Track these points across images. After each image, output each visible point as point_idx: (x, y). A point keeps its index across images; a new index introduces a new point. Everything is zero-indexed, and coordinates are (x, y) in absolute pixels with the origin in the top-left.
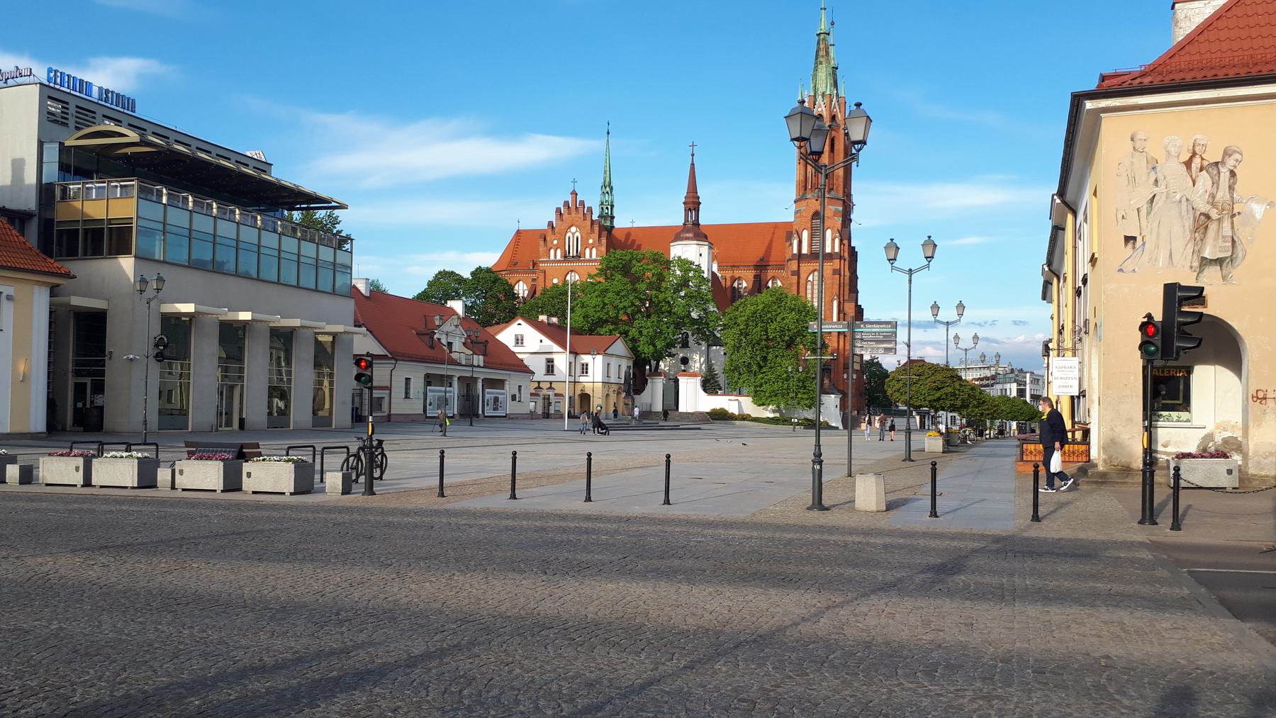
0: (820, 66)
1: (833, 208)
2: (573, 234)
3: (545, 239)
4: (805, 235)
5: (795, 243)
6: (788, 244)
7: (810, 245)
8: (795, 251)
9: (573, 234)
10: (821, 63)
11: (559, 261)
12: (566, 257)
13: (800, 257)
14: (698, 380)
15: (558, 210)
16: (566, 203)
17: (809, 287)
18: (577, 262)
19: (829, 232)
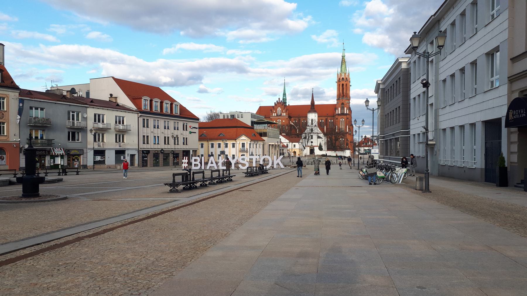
0: (343, 65)
1: (346, 102)
2: (279, 109)
3: (272, 111)
4: (339, 109)
5: (337, 111)
6: (335, 111)
7: (341, 111)
8: (337, 113)
9: (279, 109)
10: (343, 64)
11: (276, 116)
12: (277, 115)
13: (338, 114)
14: (318, 147)
15: (275, 103)
16: (277, 101)
17: (341, 122)
18: (281, 116)
19: (345, 108)
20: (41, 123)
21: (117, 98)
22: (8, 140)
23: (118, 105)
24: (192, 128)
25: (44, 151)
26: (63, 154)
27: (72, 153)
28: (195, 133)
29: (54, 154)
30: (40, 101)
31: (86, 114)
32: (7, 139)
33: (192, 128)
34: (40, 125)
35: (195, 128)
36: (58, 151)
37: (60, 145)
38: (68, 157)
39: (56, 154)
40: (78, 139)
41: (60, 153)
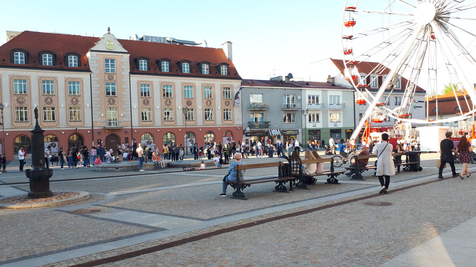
20: (259, 108)
21: (334, 78)
22: (233, 124)
23: (333, 85)
24: (416, 101)
25: (263, 132)
26: (279, 134)
27: (288, 133)
28: (422, 107)
29: (271, 135)
30: (259, 88)
31: (300, 96)
32: (215, 123)
33: (416, 101)
34: (258, 109)
35: (420, 101)
36: (275, 132)
37: (276, 126)
38: (285, 138)
39: (273, 135)
40: (293, 120)
41: (277, 134)
